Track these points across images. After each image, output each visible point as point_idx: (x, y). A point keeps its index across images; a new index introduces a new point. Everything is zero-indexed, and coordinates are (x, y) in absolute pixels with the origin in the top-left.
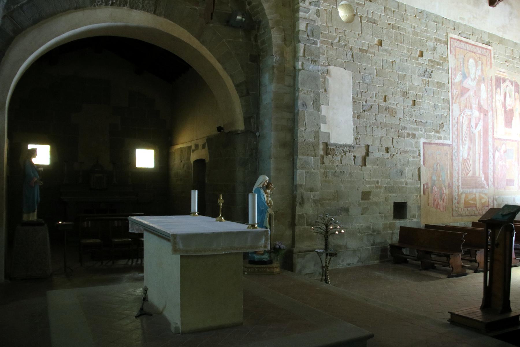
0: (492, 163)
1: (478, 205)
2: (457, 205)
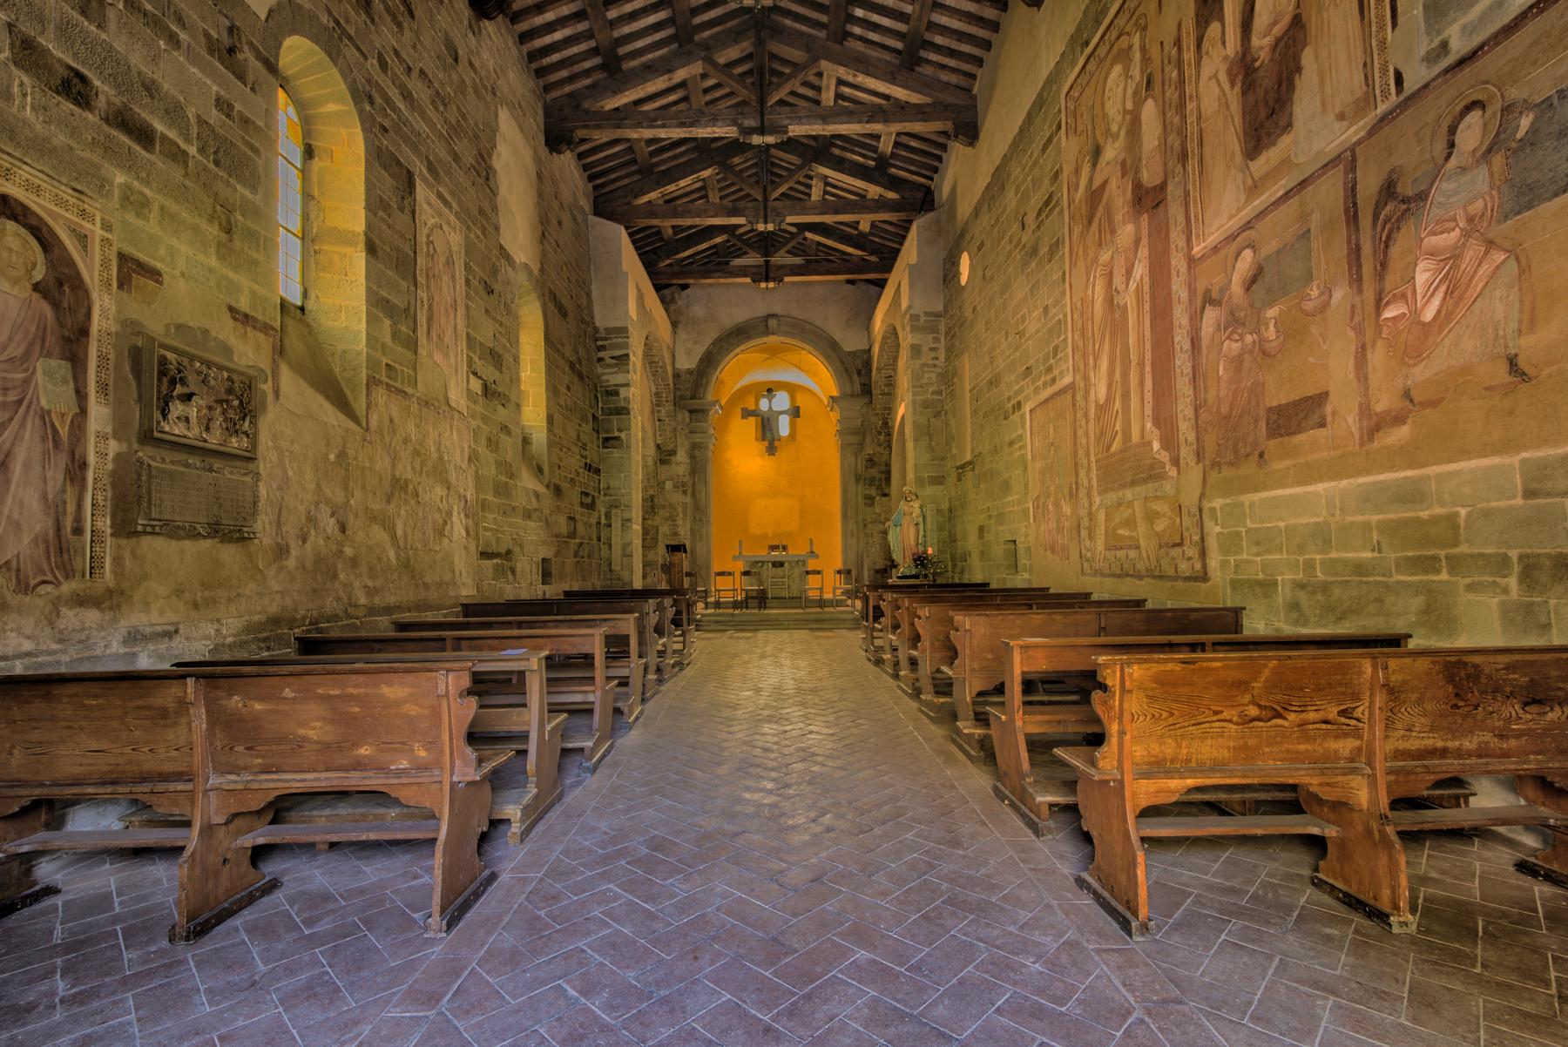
0: (1187, 368)
1: (1142, 543)
2: (1087, 542)
